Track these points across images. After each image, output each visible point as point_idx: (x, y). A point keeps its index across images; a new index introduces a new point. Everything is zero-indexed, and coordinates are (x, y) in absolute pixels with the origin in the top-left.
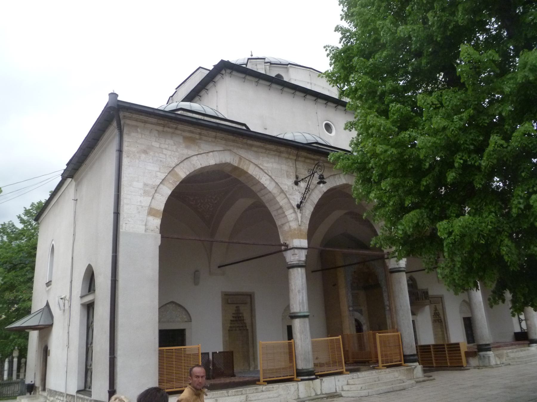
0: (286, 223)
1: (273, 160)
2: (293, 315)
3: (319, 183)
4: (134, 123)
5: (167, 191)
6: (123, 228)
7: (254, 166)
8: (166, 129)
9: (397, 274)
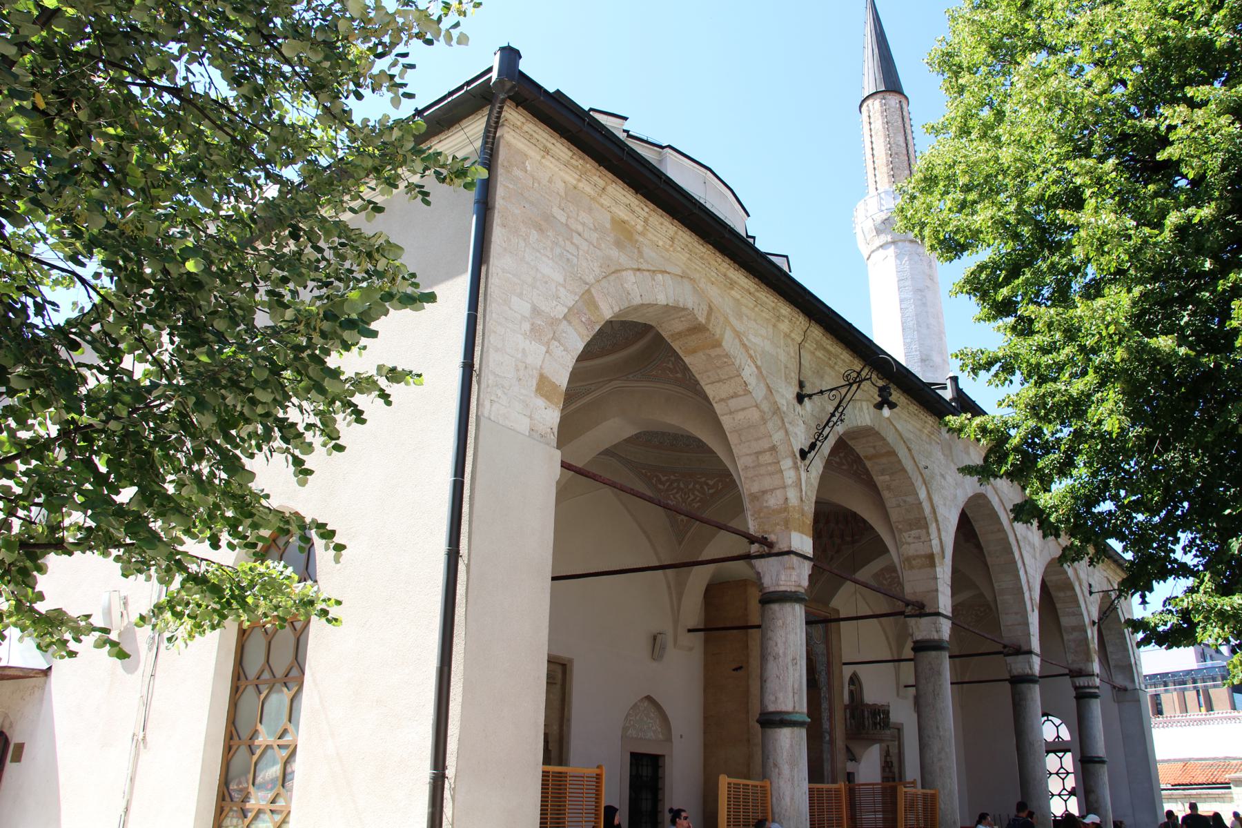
0: (772, 490)
3: (879, 406)
5: (578, 344)
9: (934, 653)
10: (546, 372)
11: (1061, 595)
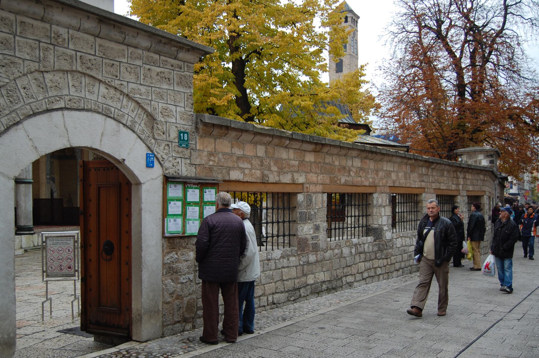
2: (20, 180)
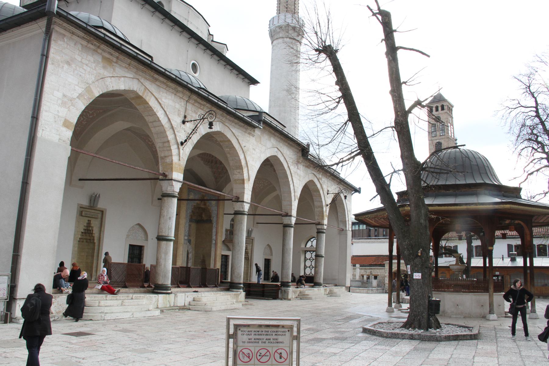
0: (168, 156)
1: (170, 97)
4: (62, 31)
5: (82, 106)
6: (41, 133)
7: (155, 99)
8: (90, 45)
9: (240, 216)
10: (67, 118)
11: (315, 194)
